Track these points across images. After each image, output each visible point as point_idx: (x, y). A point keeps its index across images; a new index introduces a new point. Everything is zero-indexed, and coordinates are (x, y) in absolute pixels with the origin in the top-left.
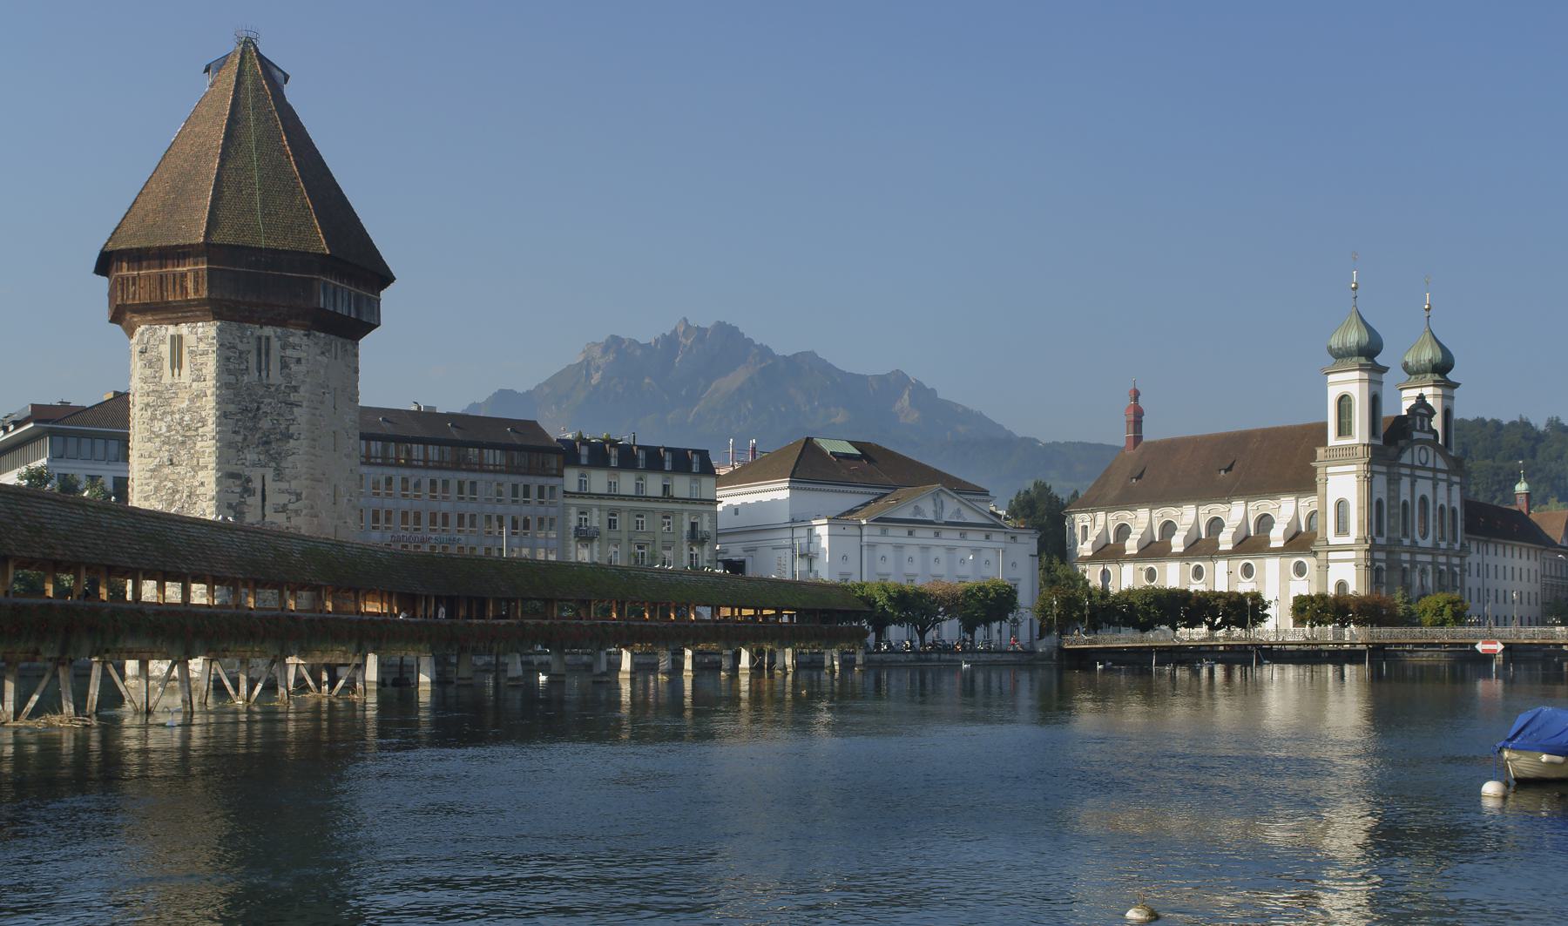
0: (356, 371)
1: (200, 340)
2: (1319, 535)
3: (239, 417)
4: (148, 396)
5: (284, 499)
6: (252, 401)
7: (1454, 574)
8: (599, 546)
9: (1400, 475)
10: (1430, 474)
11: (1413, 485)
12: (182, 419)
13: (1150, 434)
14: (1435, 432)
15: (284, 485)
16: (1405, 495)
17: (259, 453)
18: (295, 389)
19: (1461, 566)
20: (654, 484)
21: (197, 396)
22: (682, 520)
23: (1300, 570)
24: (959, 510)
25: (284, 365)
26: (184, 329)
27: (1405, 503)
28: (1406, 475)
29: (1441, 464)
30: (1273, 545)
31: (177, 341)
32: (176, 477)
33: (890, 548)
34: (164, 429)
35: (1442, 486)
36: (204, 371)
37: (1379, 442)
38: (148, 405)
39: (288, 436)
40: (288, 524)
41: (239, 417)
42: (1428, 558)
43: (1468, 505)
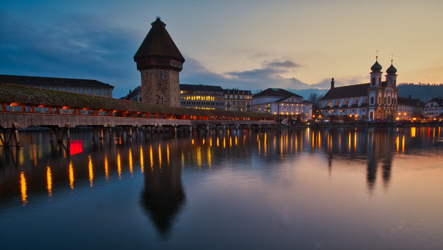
0: (179, 77)
2: (368, 104)
3: (158, 85)
4: (143, 82)
5: (166, 99)
6: (160, 83)
7: (395, 111)
8: (231, 108)
9: (385, 92)
10: (391, 92)
11: (387, 94)
12: (148, 86)
13: (336, 86)
14: (391, 84)
16: (385, 96)
17: (161, 92)
18: (167, 80)
19: (396, 109)
20: (241, 97)
21: (151, 82)
22: (246, 103)
24: (297, 100)
25: (165, 76)
26: (148, 70)
27: (385, 98)
28: (386, 92)
29: (393, 90)
30: (358, 106)
32: (148, 96)
33: (284, 107)
35: (393, 95)
36: (152, 77)
37: (380, 86)
39: (166, 89)
40: (167, 104)
41: (158, 85)
42: (389, 108)
43: (398, 98)
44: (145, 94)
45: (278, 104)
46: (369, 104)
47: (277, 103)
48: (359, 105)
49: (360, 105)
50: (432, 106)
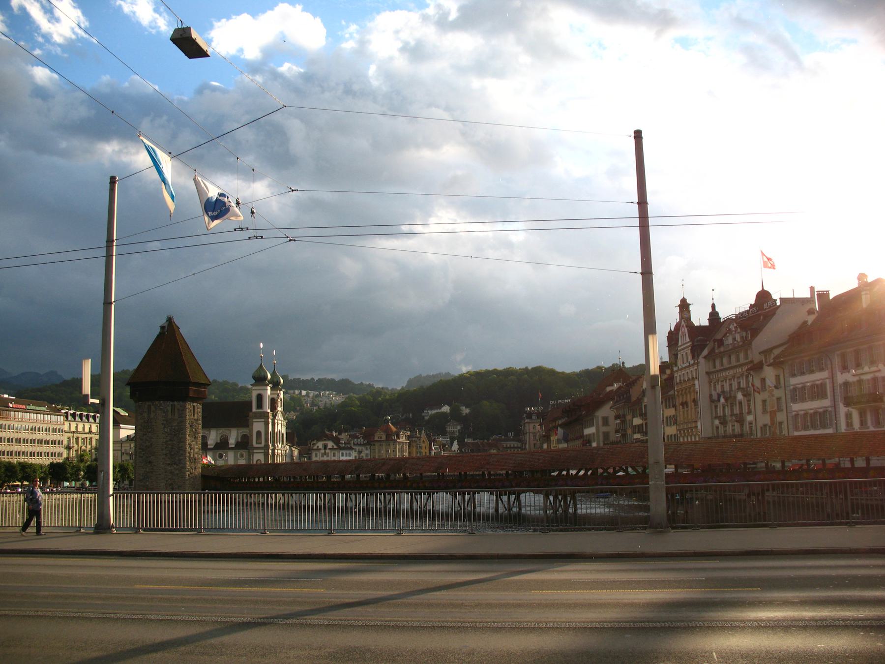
1: (181, 406)
2: (250, 444)
4: (163, 420)
11: (278, 425)
15: (197, 447)
16: (276, 430)
23: (242, 456)
25: (197, 414)
26: (176, 403)
29: (283, 419)
31: (173, 407)
34: (169, 430)
38: (163, 424)
44: (167, 441)
46: (253, 445)
48: (232, 444)
49: (234, 446)
50: (325, 447)
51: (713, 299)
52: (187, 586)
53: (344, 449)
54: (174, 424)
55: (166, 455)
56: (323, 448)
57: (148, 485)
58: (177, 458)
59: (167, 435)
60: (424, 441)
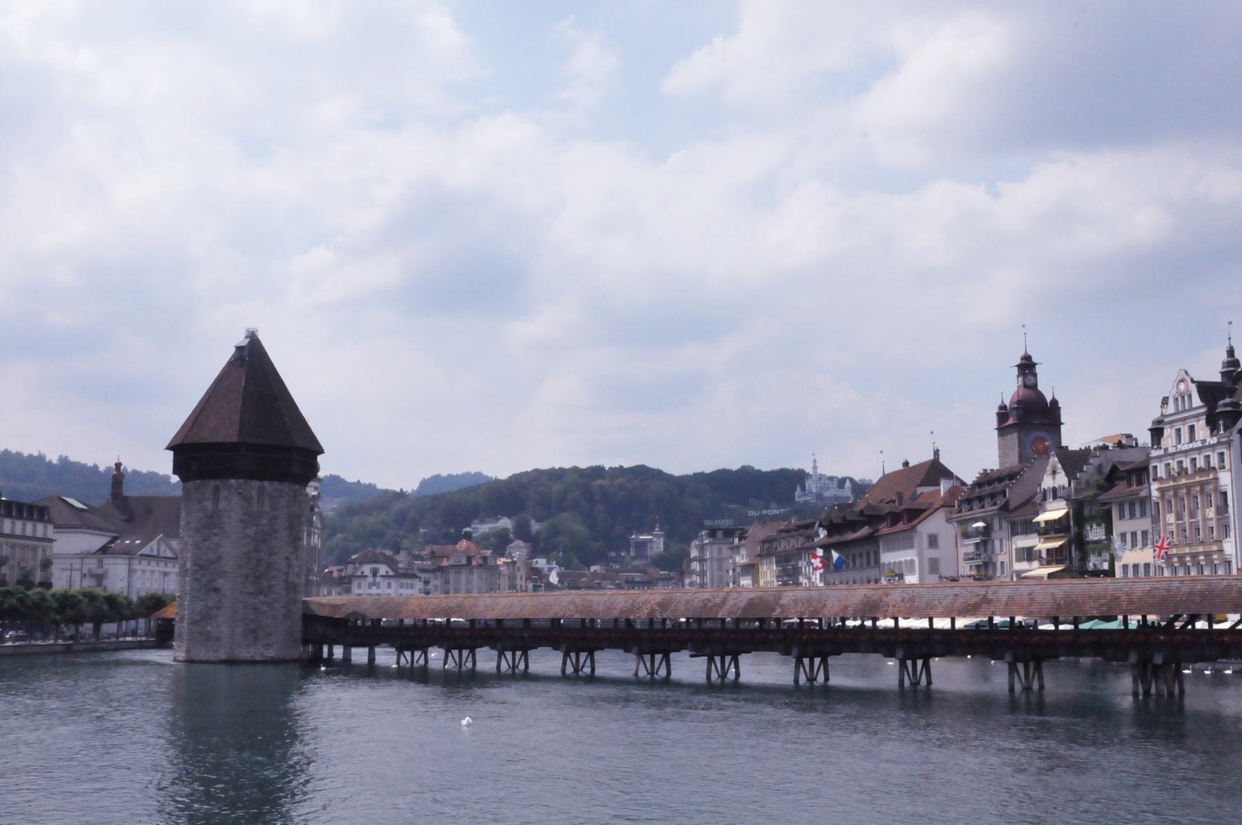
4: (243, 515)
26: (266, 484)
31: (261, 491)
34: (252, 533)
44: (249, 552)
45: (130, 559)
47: (128, 556)
50: (375, 573)
51: (1230, 339)
52: (182, 797)
53: (405, 576)
54: (264, 522)
55: (247, 576)
56: (371, 575)
57: (209, 632)
58: (265, 583)
59: (248, 540)
60: (519, 568)
